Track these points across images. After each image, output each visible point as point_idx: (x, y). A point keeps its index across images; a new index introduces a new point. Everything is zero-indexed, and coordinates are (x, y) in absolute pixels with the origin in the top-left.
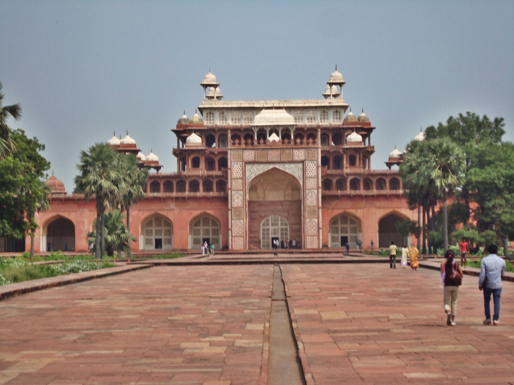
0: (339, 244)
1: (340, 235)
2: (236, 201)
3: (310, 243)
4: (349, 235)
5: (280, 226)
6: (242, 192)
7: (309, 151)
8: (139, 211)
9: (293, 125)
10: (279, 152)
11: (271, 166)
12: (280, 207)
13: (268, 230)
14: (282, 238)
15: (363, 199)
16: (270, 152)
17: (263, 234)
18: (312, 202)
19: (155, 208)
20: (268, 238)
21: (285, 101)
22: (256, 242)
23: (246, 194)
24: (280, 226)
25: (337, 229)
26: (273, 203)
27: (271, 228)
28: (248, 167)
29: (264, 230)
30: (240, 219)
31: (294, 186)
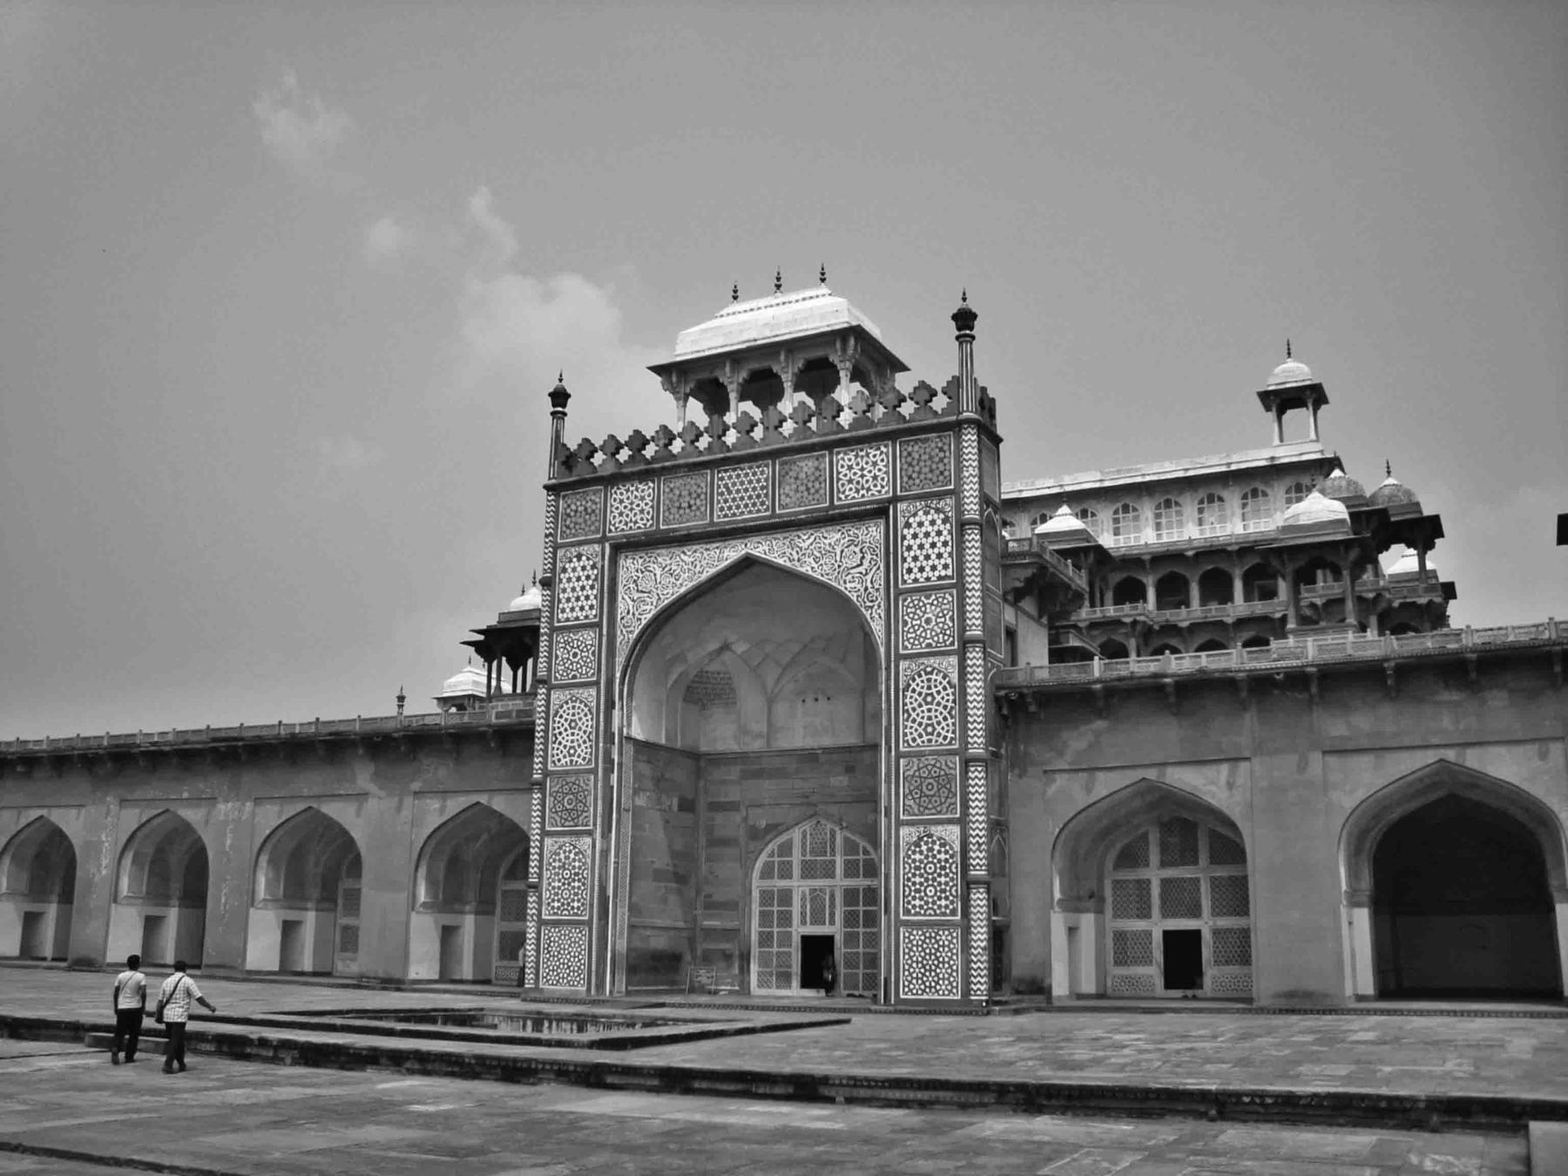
0: (1153, 972)
1: (1157, 926)
2: (566, 739)
3: (917, 970)
4: (1205, 924)
5: (840, 882)
6: (593, 691)
8: (258, 801)
10: (768, 471)
11: (732, 553)
12: (840, 781)
14: (851, 939)
15: (1245, 709)
16: (728, 477)
17: (765, 917)
19: (307, 788)
20: (786, 939)
21: (1119, 471)
22: (727, 957)
23: (610, 705)
24: (840, 882)
25: (1144, 885)
26: (809, 757)
27: (799, 886)
28: (629, 566)
29: (766, 897)
30: (578, 834)
31: (842, 647)
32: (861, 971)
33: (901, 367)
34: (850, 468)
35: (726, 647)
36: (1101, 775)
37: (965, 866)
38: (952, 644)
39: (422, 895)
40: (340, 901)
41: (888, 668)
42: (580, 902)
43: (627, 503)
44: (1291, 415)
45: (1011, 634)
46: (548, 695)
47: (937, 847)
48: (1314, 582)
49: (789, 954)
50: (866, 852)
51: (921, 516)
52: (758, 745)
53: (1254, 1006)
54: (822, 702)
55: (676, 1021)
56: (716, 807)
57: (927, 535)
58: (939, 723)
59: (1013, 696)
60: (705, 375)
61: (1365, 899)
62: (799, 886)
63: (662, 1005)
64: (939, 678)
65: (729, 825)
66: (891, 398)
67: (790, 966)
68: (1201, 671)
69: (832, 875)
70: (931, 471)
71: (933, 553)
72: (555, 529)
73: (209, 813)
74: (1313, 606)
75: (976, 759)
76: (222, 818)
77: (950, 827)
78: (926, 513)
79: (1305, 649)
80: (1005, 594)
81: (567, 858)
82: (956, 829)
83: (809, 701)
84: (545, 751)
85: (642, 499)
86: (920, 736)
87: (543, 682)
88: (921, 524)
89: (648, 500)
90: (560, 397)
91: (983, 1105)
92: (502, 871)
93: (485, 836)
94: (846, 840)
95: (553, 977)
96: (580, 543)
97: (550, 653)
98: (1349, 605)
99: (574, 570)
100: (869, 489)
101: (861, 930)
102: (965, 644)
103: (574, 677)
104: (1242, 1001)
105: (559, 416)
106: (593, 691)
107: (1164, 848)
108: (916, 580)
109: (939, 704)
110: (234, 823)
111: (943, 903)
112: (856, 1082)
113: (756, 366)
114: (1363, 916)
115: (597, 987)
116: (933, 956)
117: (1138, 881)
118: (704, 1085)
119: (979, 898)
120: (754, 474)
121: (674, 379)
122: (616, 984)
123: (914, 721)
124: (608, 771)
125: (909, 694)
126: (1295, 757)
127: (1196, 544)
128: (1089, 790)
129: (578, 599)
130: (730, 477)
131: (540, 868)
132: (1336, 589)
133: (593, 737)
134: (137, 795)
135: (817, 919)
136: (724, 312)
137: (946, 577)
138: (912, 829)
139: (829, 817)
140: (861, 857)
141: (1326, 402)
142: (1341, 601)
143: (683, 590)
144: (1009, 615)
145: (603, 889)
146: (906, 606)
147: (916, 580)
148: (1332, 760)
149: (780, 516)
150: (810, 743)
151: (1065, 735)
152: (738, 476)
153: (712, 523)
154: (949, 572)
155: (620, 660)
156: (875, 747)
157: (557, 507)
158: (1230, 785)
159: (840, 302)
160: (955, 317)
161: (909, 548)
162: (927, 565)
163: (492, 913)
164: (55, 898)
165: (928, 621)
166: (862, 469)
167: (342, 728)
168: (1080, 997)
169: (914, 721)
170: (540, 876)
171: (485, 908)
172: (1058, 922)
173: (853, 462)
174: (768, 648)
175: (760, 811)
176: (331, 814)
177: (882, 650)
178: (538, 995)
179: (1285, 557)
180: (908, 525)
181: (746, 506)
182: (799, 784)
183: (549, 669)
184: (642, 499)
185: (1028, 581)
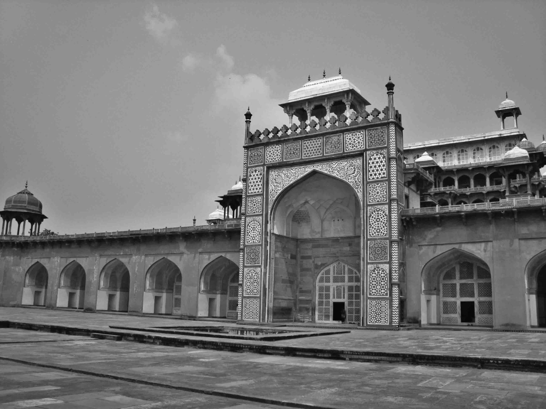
0: (457, 316)
1: (459, 300)
2: (251, 234)
3: (373, 314)
4: (476, 299)
5: (347, 284)
6: (261, 217)
7: (373, 132)
8: (146, 255)
10: (321, 140)
11: (309, 169)
12: (347, 249)
13: (328, 289)
14: (350, 303)
15: (490, 223)
16: (307, 143)
17: (321, 296)
18: (378, 230)
19: (163, 251)
20: (328, 303)
22: (307, 309)
23: (267, 222)
24: (347, 284)
26: (336, 240)
27: (332, 285)
28: (273, 174)
29: (321, 289)
31: (348, 201)
32: (354, 315)
33: (368, 103)
34: (350, 139)
35: (307, 202)
36: (439, 247)
37: (391, 278)
38: (386, 201)
39: (202, 288)
40: (174, 290)
41: (364, 209)
42: (257, 290)
43: (272, 152)
44: (507, 119)
45: (407, 197)
46: (245, 219)
47: (381, 272)
48: (516, 179)
49: (329, 309)
50: (356, 273)
51: (375, 156)
52: (318, 236)
53: (494, 328)
54: (341, 221)
55: (290, 331)
56: (303, 258)
57: (377, 162)
58: (381, 228)
59: (408, 219)
60: (299, 107)
61: (534, 292)
62: (332, 285)
63: (285, 326)
64: (382, 213)
65: (307, 264)
66: (364, 115)
67: (329, 313)
68: (475, 210)
69: (344, 281)
70: (379, 140)
71: (379, 169)
72: (247, 161)
73: (130, 260)
74: (515, 187)
75: (394, 241)
76: (134, 261)
77: (385, 265)
78: (377, 155)
80: (405, 183)
81: (252, 275)
82: (388, 265)
83: (336, 221)
84: (244, 238)
85: (277, 151)
86: (375, 233)
87: (243, 214)
88: (375, 159)
89: (279, 151)
90: (248, 116)
91: (397, 362)
92: (230, 280)
93: (223, 268)
94: (349, 269)
95: (247, 316)
96: (256, 166)
97: (246, 204)
98: (529, 187)
99: (254, 175)
100: (357, 147)
101: (354, 300)
102: (391, 200)
103: (254, 213)
104: (490, 327)
105: (248, 122)
106: (261, 217)
107: (461, 272)
108: (373, 178)
109: (381, 222)
110: (138, 262)
111: (383, 291)
112: (353, 353)
113: (317, 104)
114: (533, 297)
115: (263, 319)
116: (379, 309)
117: (452, 284)
118: (300, 353)
119: (395, 289)
120: (316, 142)
122: (269, 318)
123: (373, 228)
124: (266, 245)
125: (371, 218)
126: (509, 241)
127: (472, 165)
128: (434, 252)
129: (255, 186)
130: (308, 143)
131: (243, 278)
132: (524, 181)
133: (261, 233)
134: (106, 253)
135: (339, 297)
136: (305, 85)
137: (384, 177)
138: (372, 265)
139: (343, 261)
140: (354, 275)
141: (521, 114)
142: (526, 185)
143: (292, 182)
144: (406, 190)
145: (264, 286)
146: (370, 188)
147: (373, 178)
148: (522, 242)
149: (325, 156)
150: (337, 235)
151: (426, 233)
152: (311, 142)
153: (302, 159)
154: (385, 176)
155: (270, 207)
156: (359, 237)
157: (248, 154)
158: (485, 251)
159: (346, 81)
160: (386, 86)
161: (371, 167)
162: (377, 173)
163: (227, 294)
164: (79, 288)
165: (378, 193)
166: (354, 140)
167: (175, 230)
168: (431, 324)
169: (373, 228)
170: (243, 281)
171: (224, 292)
172: (423, 298)
173: (351, 137)
174: (322, 203)
175: (318, 259)
176: (171, 260)
177: (362, 203)
178: (243, 322)
179: (505, 170)
180: (371, 159)
181: (314, 153)
182: (332, 250)
183: (246, 210)
184: (277, 151)
185: (413, 178)
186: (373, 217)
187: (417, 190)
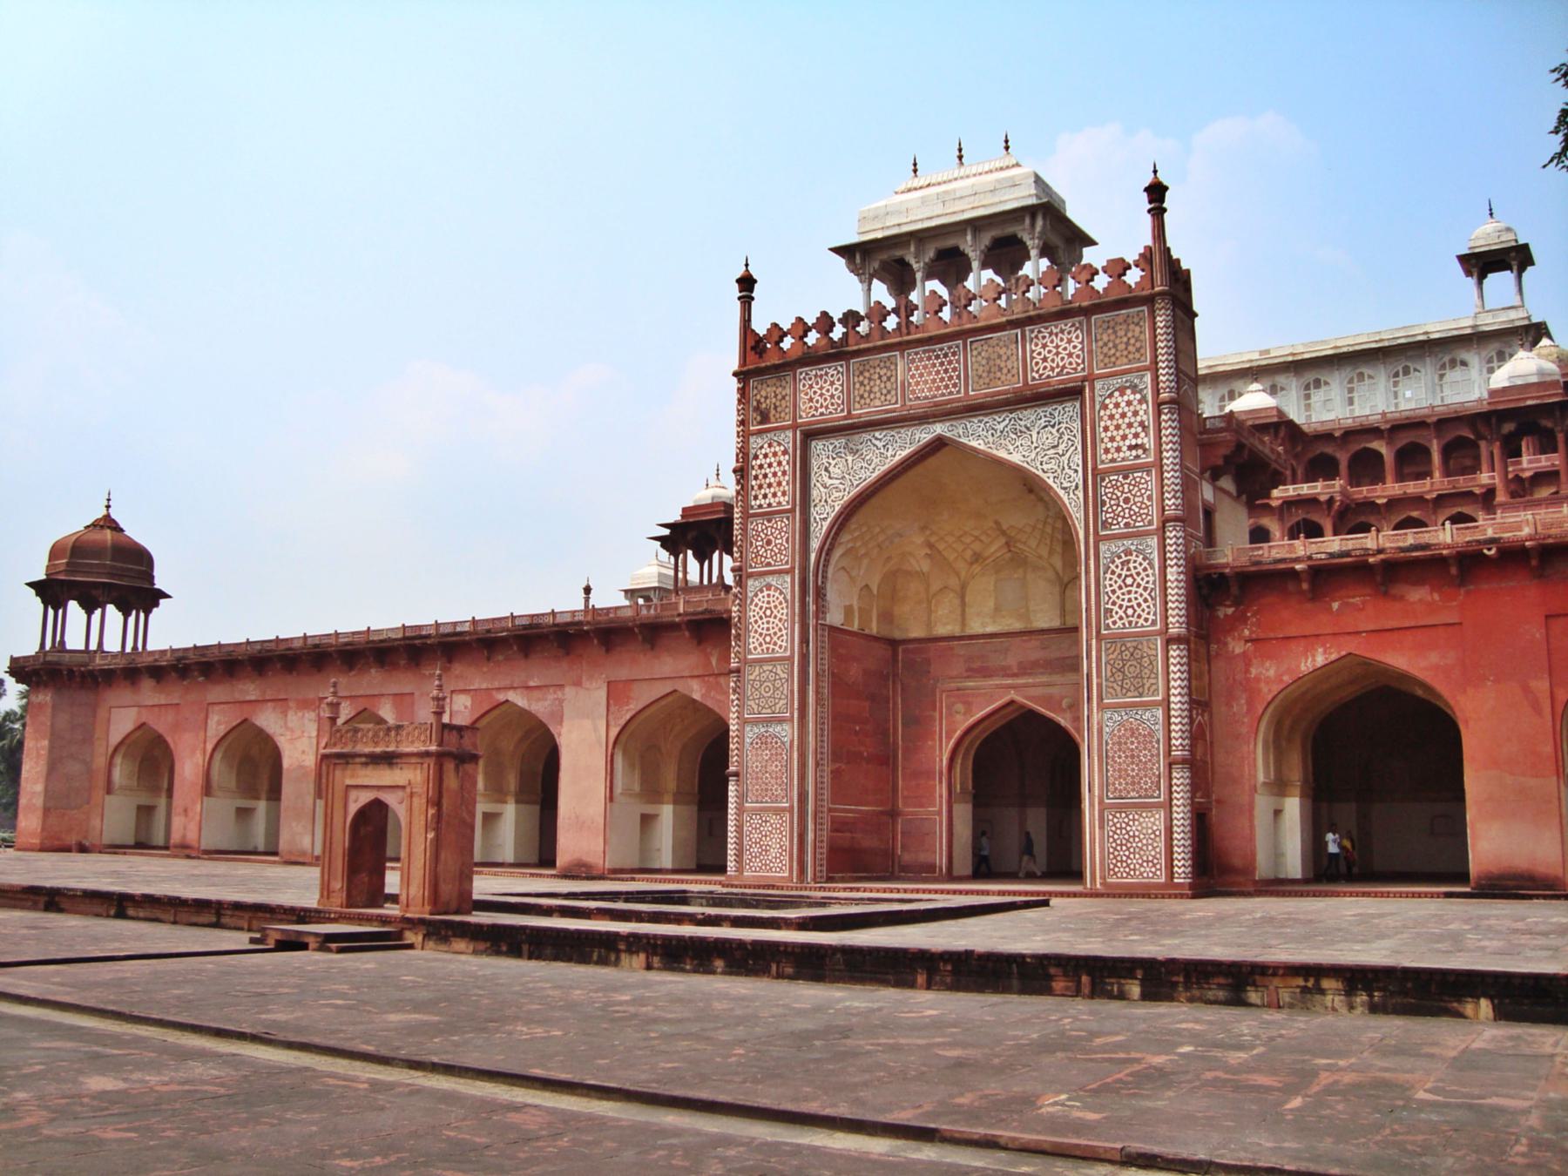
6: (788, 578)
9: (1030, 211)
33: (1092, 243)
38: (1151, 523)
45: (1209, 513)
66: (1085, 276)
79: (1520, 524)
80: (1203, 472)
82: (1160, 713)
103: (769, 564)
106: (788, 578)
121: (858, 260)
125: (1108, 576)
132: (1545, 462)
141: (1532, 264)
144: (1207, 492)
155: (815, 544)
156: (1076, 629)
160: (1146, 190)
166: (1057, 347)
172: (1263, 804)
185: (1226, 458)
186: (1113, 573)
187: (1239, 496)
